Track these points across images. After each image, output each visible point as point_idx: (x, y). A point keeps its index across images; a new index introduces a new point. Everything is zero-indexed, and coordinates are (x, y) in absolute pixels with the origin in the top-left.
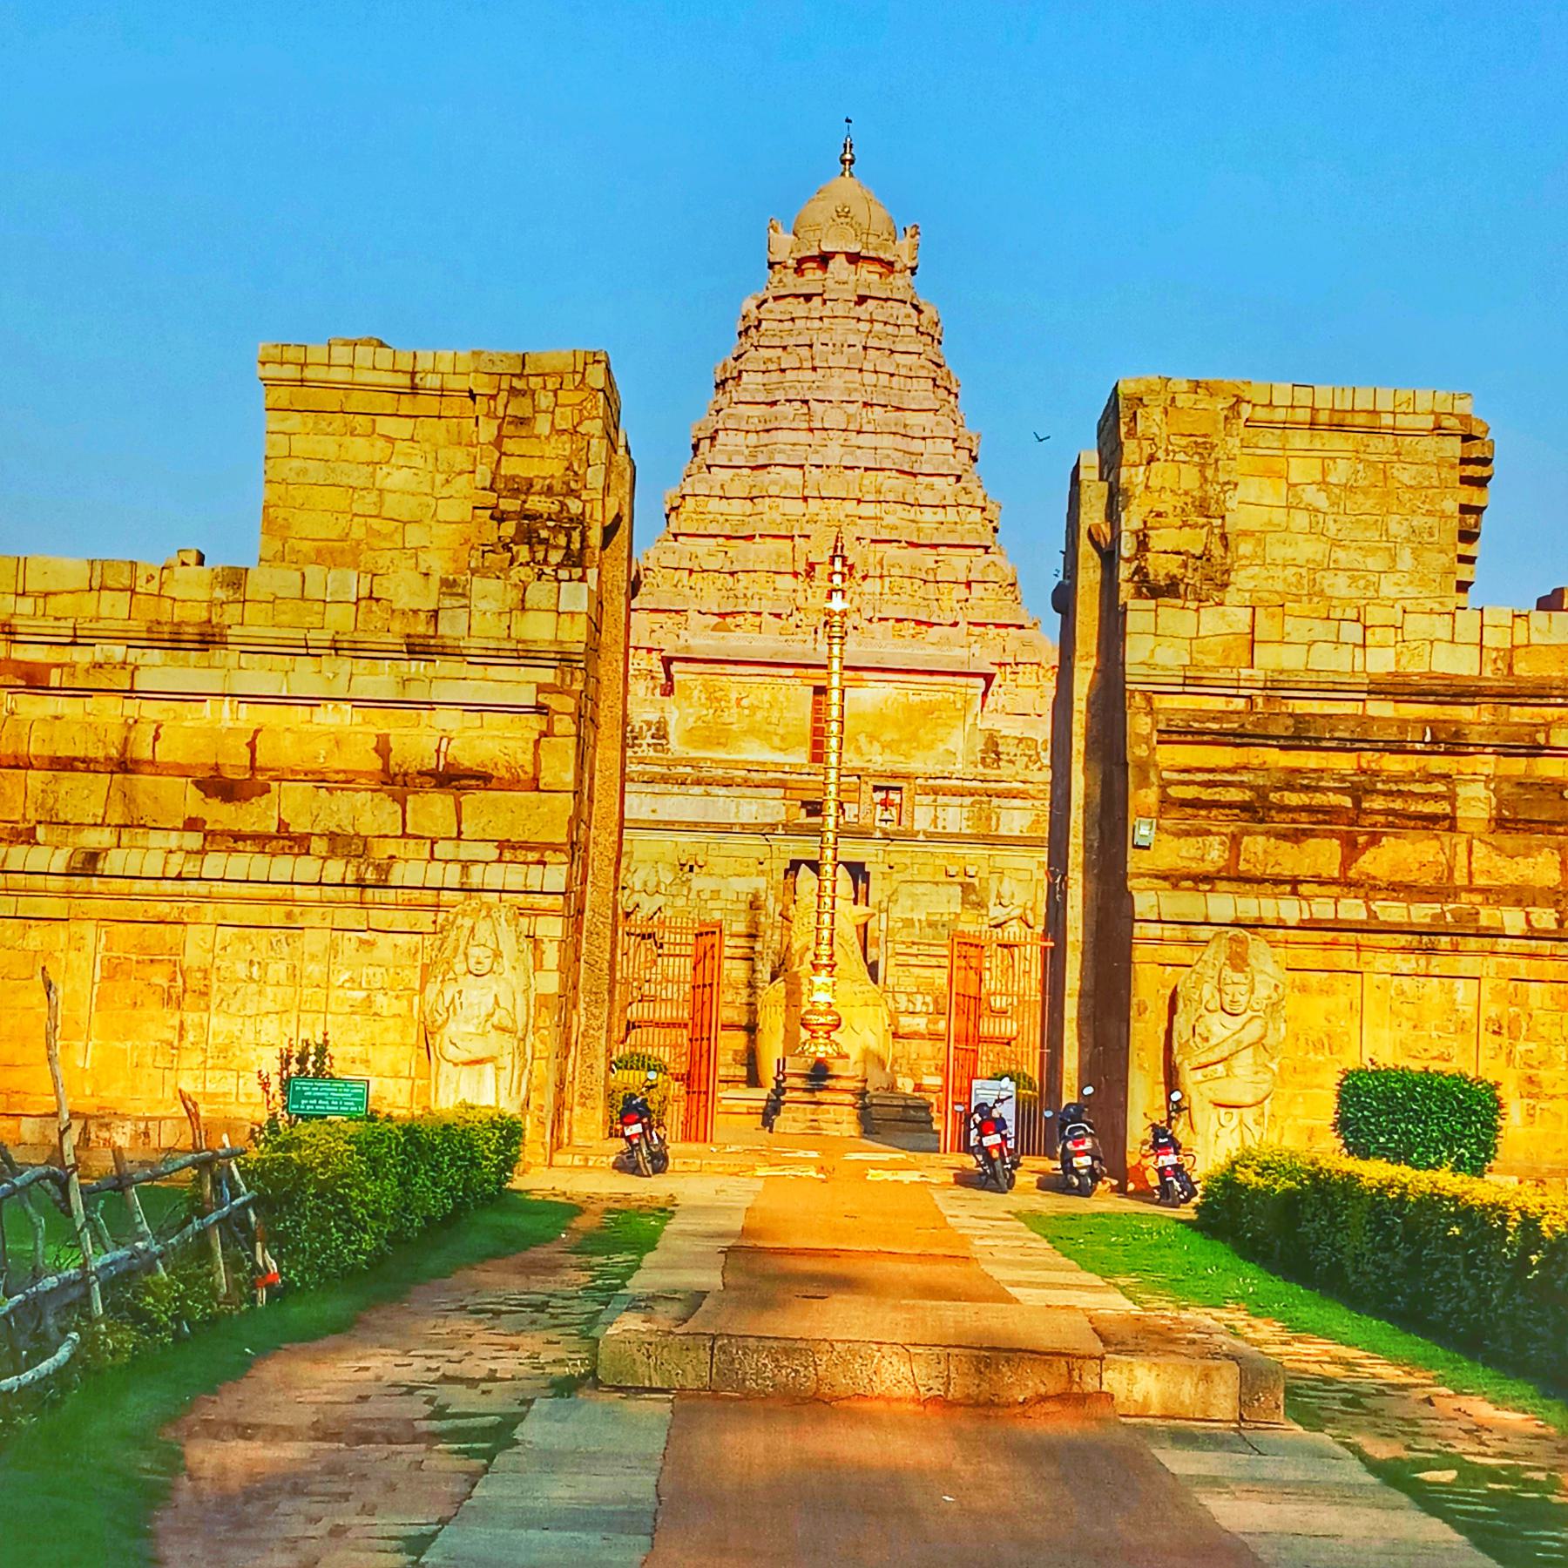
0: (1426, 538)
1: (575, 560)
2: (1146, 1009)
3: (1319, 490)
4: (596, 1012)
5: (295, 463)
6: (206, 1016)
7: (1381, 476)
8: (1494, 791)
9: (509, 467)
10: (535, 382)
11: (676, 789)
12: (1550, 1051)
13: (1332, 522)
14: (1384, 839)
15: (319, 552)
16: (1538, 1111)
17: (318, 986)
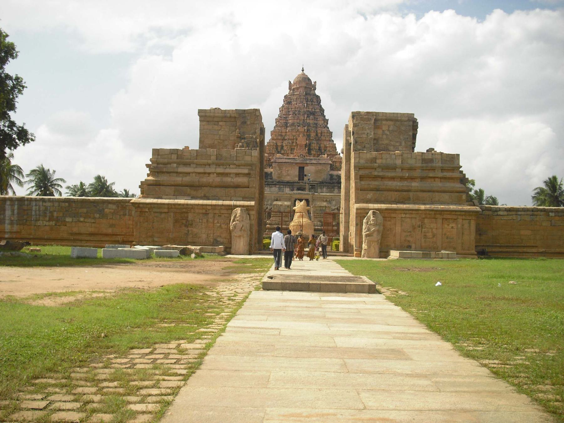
1: (255, 147)
5: (205, 130)
11: (274, 186)
15: (209, 146)
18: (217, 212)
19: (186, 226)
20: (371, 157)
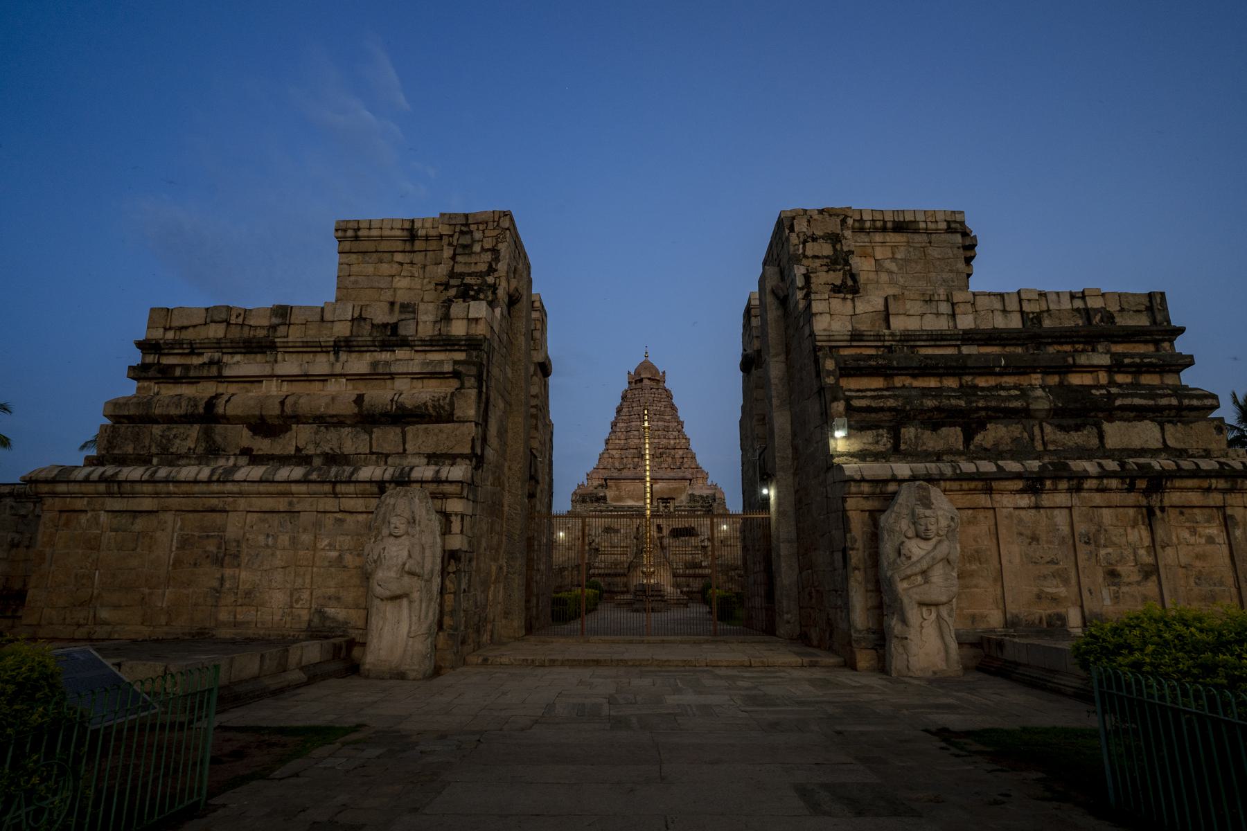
0: (951, 283)
2: (856, 541)
4: (512, 563)
5: (352, 278)
6: (237, 571)
9: (458, 269)
10: (473, 227)
12: (1122, 553)
13: (900, 279)
14: (988, 426)
16: (1121, 595)
17: (308, 549)
18: (328, 508)
19: (218, 561)
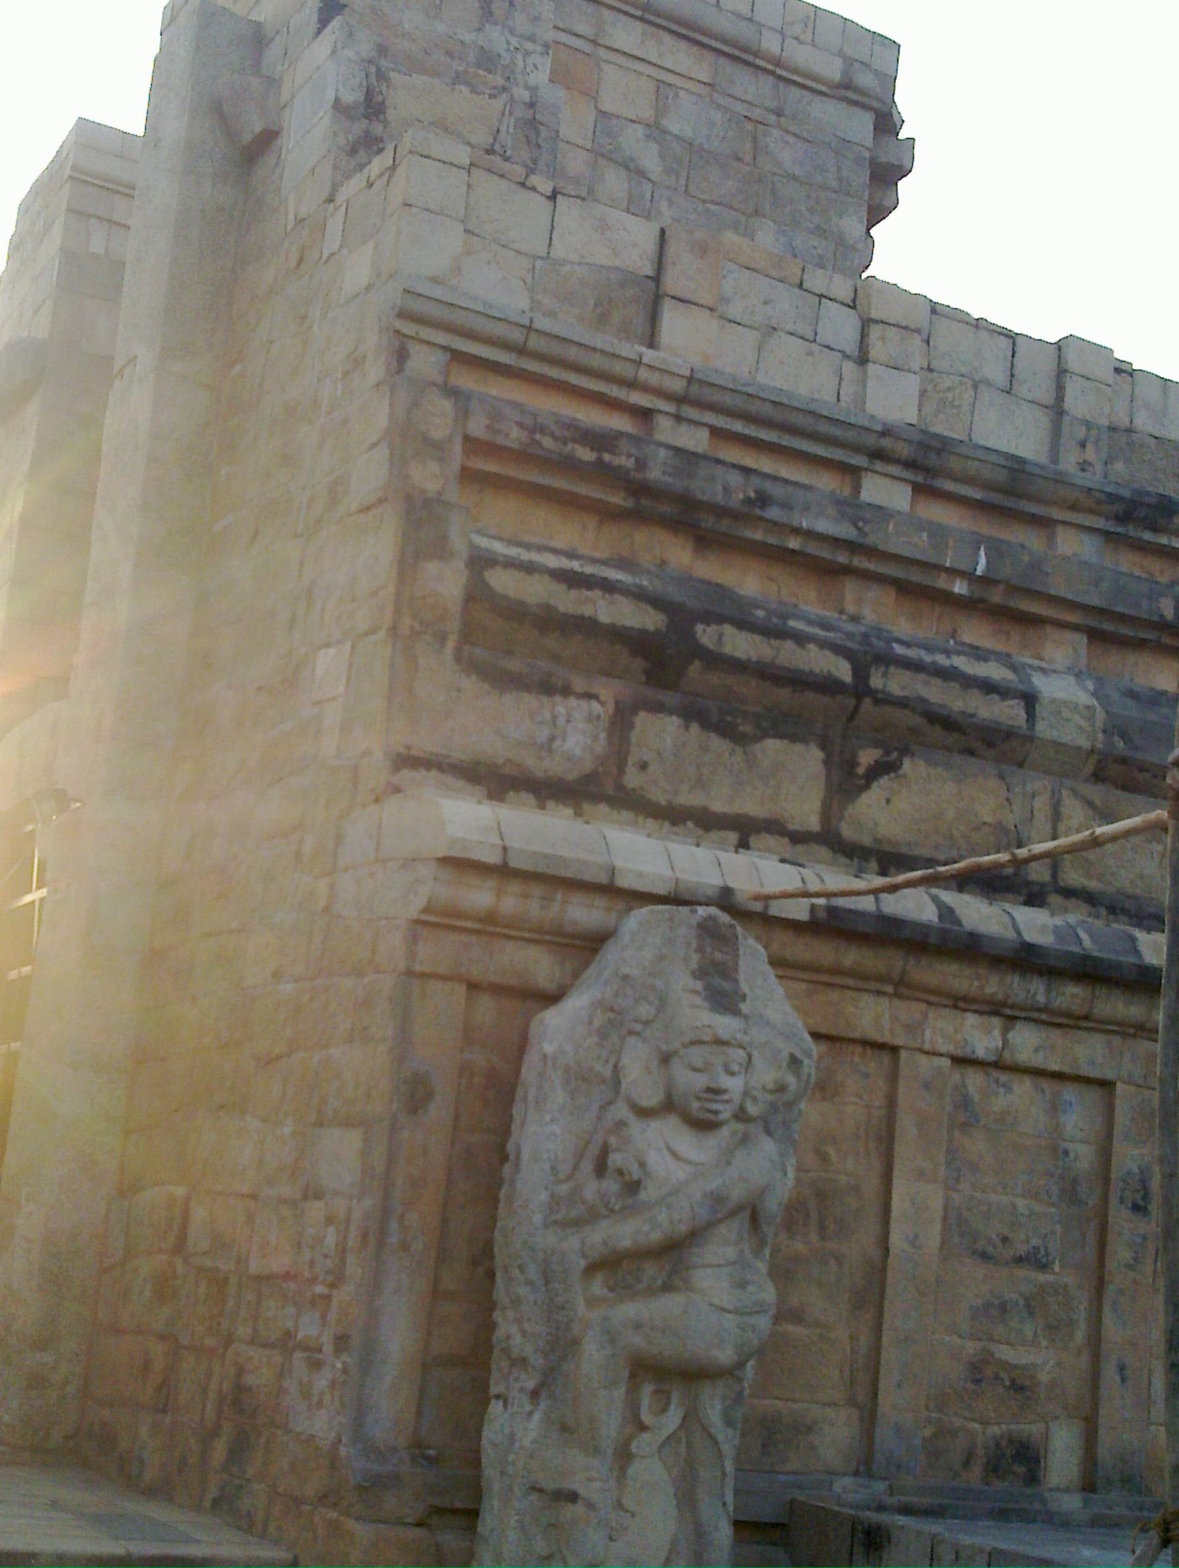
2: (429, 1096)
3: (648, 137)
7: (748, 146)
8: (1095, 694)
13: (664, 206)
14: (907, 764)
20: (603, 257)
